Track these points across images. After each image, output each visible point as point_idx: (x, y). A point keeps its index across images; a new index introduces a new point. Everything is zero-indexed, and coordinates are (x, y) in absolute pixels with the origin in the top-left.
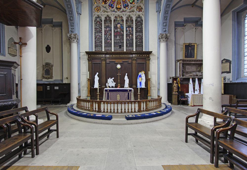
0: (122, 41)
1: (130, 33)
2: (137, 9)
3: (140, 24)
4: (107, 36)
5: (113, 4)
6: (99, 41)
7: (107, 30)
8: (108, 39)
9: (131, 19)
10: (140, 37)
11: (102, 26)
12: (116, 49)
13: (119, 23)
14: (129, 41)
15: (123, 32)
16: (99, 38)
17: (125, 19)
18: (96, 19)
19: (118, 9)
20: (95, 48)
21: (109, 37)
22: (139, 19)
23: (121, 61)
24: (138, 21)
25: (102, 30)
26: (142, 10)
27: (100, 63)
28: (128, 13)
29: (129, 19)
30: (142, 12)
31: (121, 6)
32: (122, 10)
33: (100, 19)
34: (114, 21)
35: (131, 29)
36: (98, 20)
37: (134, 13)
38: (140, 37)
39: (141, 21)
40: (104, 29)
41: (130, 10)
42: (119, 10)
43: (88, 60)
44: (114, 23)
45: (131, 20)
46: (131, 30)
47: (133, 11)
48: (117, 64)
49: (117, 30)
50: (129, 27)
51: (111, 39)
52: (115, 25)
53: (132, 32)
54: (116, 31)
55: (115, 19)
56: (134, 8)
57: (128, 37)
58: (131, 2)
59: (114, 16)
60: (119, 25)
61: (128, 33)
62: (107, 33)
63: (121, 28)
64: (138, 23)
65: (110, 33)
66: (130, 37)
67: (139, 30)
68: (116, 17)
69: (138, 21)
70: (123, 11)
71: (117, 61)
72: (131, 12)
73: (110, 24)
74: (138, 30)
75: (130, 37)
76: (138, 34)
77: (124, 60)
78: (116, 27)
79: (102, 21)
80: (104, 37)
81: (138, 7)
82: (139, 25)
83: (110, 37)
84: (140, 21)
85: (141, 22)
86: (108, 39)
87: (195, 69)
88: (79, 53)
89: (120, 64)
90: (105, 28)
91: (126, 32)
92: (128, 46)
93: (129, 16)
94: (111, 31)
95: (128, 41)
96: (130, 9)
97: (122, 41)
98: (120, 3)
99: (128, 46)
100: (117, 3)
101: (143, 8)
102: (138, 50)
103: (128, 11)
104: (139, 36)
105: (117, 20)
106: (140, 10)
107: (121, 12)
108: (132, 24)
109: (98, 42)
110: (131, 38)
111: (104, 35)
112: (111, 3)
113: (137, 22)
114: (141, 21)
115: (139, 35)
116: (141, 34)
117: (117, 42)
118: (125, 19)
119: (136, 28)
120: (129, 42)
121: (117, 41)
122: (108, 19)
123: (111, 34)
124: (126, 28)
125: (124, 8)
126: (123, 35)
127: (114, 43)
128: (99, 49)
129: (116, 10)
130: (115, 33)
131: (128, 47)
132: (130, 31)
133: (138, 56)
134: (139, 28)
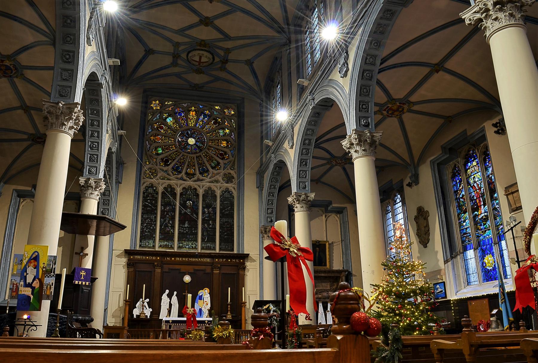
1: (209, 217)
2: (223, 178)
4: (166, 220)
5: (181, 166)
7: (166, 210)
8: (166, 226)
9: (212, 194)
10: (228, 226)
13: (189, 200)
14: (207, 231)
15: (197, 214)
17: (201, 192)
18: (147, 190)
19: (190, 176)
20: (141, 241)
21: (170, 223)
22: (226, 195)
23: (191, 268)
26: (233, 180)
27: (151, 272)
28: (208, 184)
29: (210, 194)
30: (233, 183)
31: (194, 170)
32: (195, 178)
34: (181, 194)
35: (213, 211)
36: (150, 190)
37: (218, 185)
39: (231, 197)
40: (161, 208)
41: (210, 178)
46: (212, 212)
47: (217, 181)
48: (185, 274)
51: (173, 227)
54: (183, 212)
55: (182, 191)
56: (218, 176)
57: (206, 225)
58: (213, 165)
59: (181, 187)
60: (191, 202)
61: (205, 217)
63: (193, 208)
66: (210, 225)
70: (198, 180)
71: (183, 268)
72: (212, 182)
76: (224, 220)
77: (197, 268)
81: (225, 174)
87: (329, 286)
88: (111, 250)
89: (189, 274)
90: (162, 205)
93: (210, 188)
95: (205, 231)
96: (210, 178)
97: (193, 231)
98: (194, 166)
100: (188, 165)
101: (235, 176)
102: (225, 248)
103: (209, 180)
105: (187, 193)
106: (229, 179)
107: (195, 181)
110: (211, 226)
112: (177, 164)
114: (231, 199)
115: (226, 222)
118: (201, 192)
120: (208, 233)
122: (170, 191)
123: (173, 218)
124: (203, 208)
126: (196, 222)
127: (179, 233)
131: (206, 242)
133: (223, 260)
134: (226, 209)
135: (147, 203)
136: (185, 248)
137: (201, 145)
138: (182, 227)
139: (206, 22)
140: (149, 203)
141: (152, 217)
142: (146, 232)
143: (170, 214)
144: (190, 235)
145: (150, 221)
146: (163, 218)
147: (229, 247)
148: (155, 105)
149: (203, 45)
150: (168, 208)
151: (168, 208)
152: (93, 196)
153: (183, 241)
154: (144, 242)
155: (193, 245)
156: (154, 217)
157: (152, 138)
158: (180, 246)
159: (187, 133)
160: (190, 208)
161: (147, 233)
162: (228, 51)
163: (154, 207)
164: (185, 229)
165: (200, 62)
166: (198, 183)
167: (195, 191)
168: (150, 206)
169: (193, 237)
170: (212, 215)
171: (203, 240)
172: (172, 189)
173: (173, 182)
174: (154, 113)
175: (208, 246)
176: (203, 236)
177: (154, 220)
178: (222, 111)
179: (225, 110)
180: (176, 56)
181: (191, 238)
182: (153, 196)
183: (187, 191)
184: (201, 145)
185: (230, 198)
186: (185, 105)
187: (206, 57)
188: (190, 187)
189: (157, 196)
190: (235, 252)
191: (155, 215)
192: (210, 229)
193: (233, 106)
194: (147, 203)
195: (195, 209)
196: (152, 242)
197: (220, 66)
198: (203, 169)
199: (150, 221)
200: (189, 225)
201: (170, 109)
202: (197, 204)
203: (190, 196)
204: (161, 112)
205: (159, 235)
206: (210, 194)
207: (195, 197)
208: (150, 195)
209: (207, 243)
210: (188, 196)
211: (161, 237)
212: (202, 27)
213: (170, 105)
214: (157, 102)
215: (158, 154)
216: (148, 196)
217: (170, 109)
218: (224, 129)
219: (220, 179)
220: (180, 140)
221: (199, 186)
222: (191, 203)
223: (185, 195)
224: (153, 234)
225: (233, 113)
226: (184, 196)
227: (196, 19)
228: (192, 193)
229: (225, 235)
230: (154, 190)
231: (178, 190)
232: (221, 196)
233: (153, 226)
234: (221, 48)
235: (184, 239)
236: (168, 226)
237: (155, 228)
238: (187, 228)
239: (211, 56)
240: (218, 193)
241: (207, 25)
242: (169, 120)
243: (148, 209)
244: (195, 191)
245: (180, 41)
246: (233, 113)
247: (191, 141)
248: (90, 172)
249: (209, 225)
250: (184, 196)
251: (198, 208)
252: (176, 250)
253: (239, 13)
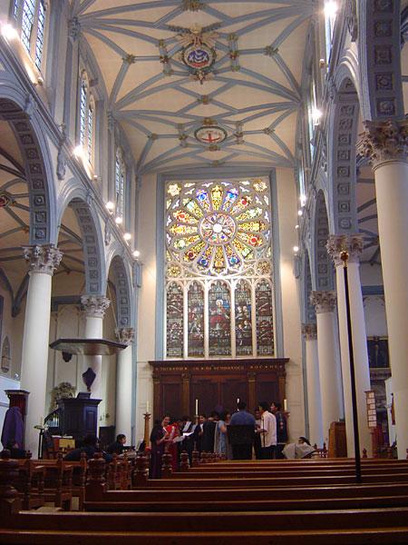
1: (243, 316)
11: (182, 304)
13: (219, 298)
14: (242, 333)
15: (229, 315)
17: (233, 287)
19: (219, 269)
22: (263, 288)
27: (178, 385)
32: (225, 271)
33: (179, 291)
34: (210, 293)
36: (175, 291)
42: (219, 270)
43: (154, 377)
50: (242, 304)
64: (261, 295)
68: (213, 285)
70: (229, 272)
72: (244, 274)
76: (261, 319)
78: (213, 306)
79: (182, 294)
86: (195, 331)
88: (135, 363)
91: (236, 315)
94: (203, 314)
103: (240, 272)
107: (225, 275)
116: (268, 319)
118: (233, 287)
119: (257, 307)
124: (236, 306)
125: (231, 265)
126: (229, 322)
127: (210, 338)
129: (213, 272)
132: (243, 312)
137: (229, 231)
139: (205, 100)
148: (173, 190)
149: (208, 123)
150: (196, 310)
151: (196, 310)
152: (96, 315)
157: (173, 229)
159: (212, 219)
162: (239, 124)
165: (210, 140)
166: (229, 277)
168: (176, 310)
171: (237, 344)
173: (198, 279)
174: (173, 199)
178: (251, 187)
179: (256, 186)
180: (183, 137)
184: (229, 231)
186: (207, 186)
187: (216, 135)
188: (219, 281)
190: (276, 357)
193: (263, 178)
197: (235, 139)
198: (234, 261)
201: (191, 192)
204: (180, 198)
206: (243, 289)
212: (202, 105)
213: (192, 187)
214: (176, 186)
215: (180, 248)
216: (172, 298)
217: (191, 192)
218: (254, 208)
219: (255, 269)
220: (204, 228)
225: (265, 187)
227: (193, 100)
230: (179, 291)
231: (207, 287)
232: (256, 292)
234: (230, 122)
239: (222, 132)
240: (253, 287)
241: (206, 103)
242: (191, 206)
245: (182, 122)
246: (265, 187)
247: (217, 228)
248: (92, 290)
249: (244, 326)
252: (207, 358)
253: (238, 87)
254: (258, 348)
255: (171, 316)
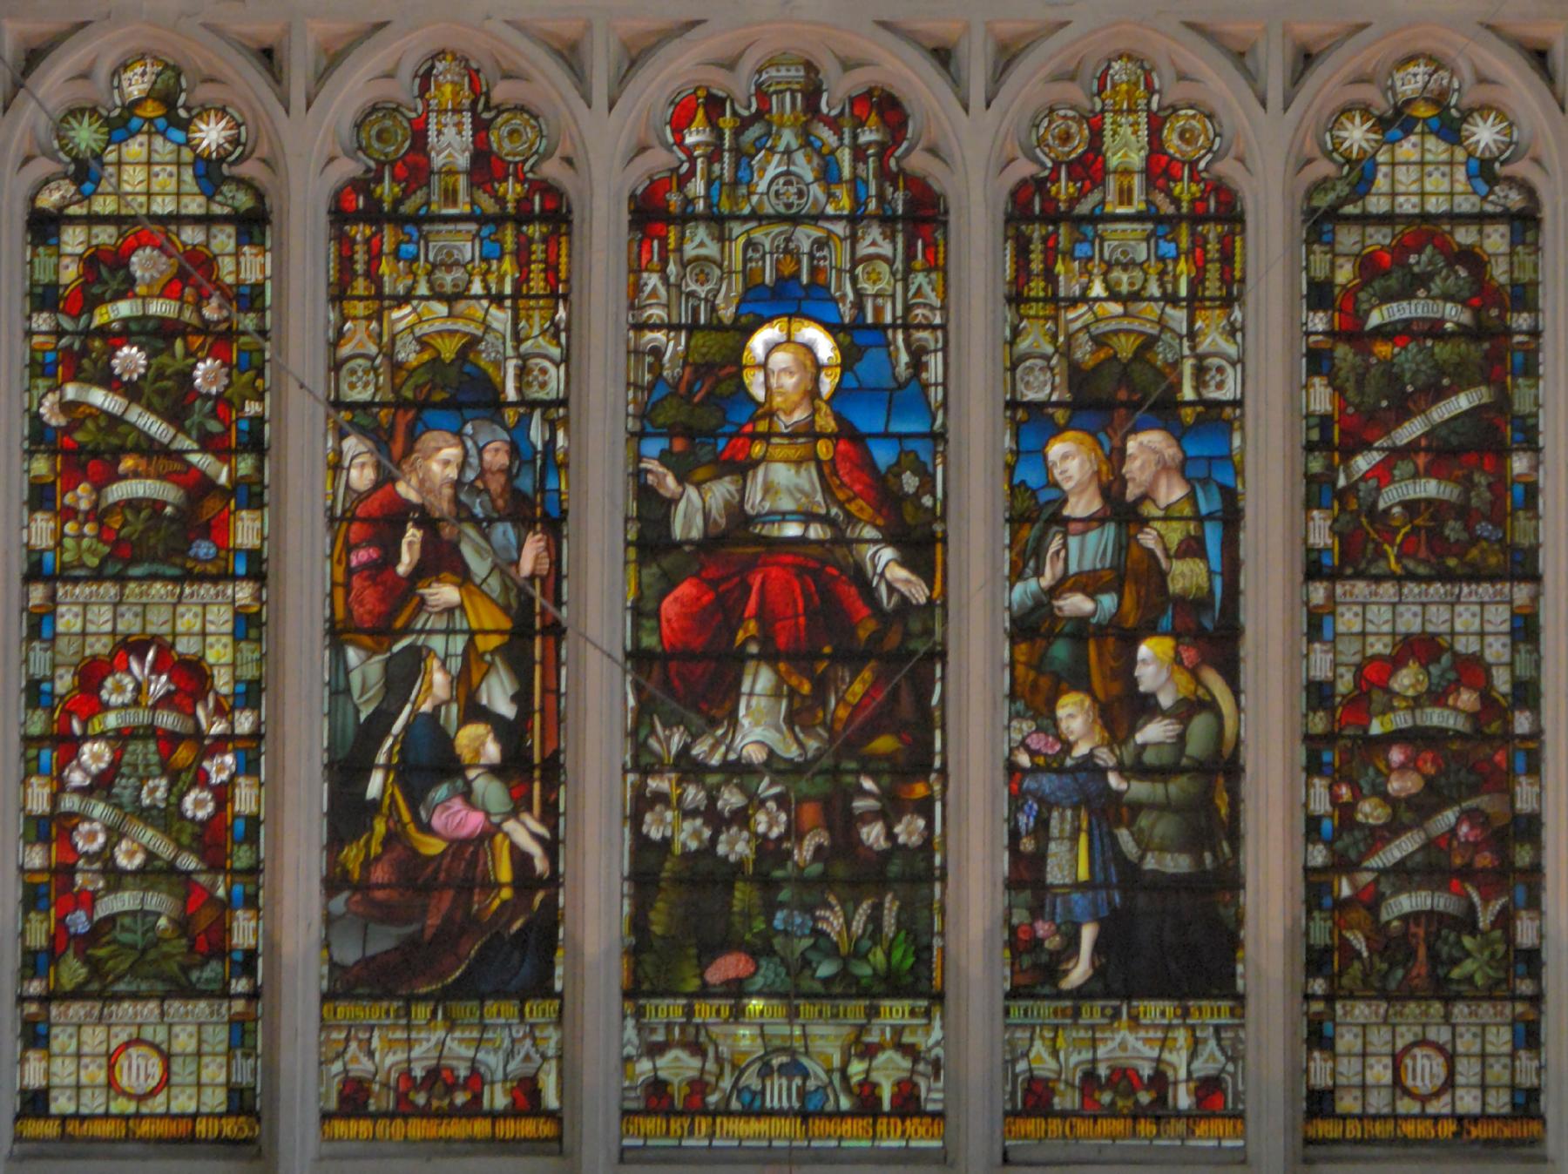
0: (890, 812)
3: (1454, 314)
4: (415, 661)
6: (168, 818)
7: (407, 490)
9: (1159, 169)
10: (1435, 717)
12: (678, 1066)
16: (167, 720)
18: (84, 172)
21: (474, 711)
24: (1380, 237)
25: (251, 494)
38: (1437, 697)
39: (1480, 219)
44: (636, 270)
45: (1185, 189)
46: (1172, 492)
49: (720, 491)
52: (672, 346)
53: (1193, 548)
54: (687, 522)
55: (659, 160)
57: (1073, 714)
61: (1062, 585)
62: (427, 570)
65: (505, 565)
67: (1429, 488)
69: (1387, 219)
73: (500, 318)
74: (1391, 497)
75: (1146, 707)
80: (339, 690)
82: (1435, 330)
83: (499, 695)
84: (1455, 218)
85: (1473, 259)
91: (1026, 559)
92: (1079, 972)
97: (873, 834)
99: (1079, 972)
104: (1406, 680)
108: (1195, 302)
109: (127, 859)
110: (1154, 732)
111: (338, 635)
113: (1369, 266)
115: (1420, 647)
117: (736, 846)
120: (1105, 851)
121: (741, 818)
128: (139, 1070)
130: (669, 582)
131: (1081, 994)
134: (1411, 430)
135: (99, 397)
136: (748, 1113)
138: (689, 769)
140: (131, 391)
141: (188, 620)
142: (116, 878)
143: (479, 566)
144: (813, 890)
145: (160, 685)
146: (381, 632)
147: (1467, 1071)
153: (705, 992)
154: (94, 1039)
155: (869, 1052)
156: (221, 618)
158: (657, 1087)
160: (809, 432)
161: (125, 901)
163: (223, 452)
164: (731, 799)
167: (884, 150)
168: (150, 449)
169: (875, 918)
170: (1175, 534)
172: (499, 140)
175: (1123, 1078)
176: (1037, 912)
177: (223, 682)
181: (833, 951)
182: (200, 263)
183: (740, 154)
185: (1464, 236)
189: (251, 276)
191: (244, 593)
192: (1140, 789)
194: (99, 397)
195: (883, 455)
196: (218, 1037)
199: (166, 701)
200: (796, 719)
202: (917, 365)
203: (805, 237)
205: (329, 920)
207: (874, 241)
208: (144, 264)
209: (1093, 1012)
210: (766, 236)
211: (349, 954)
221: (943, 56)
222: (826, 348)
223: (717, 221)
224: (227, 905)
226: (699, 242)
228: (828, 174)
229: (1404, 875)
233: (221, 767)
235: (728, 967)
236: (449, 766)
237: (245, 799)
238: (767, 788)
243: (118, 491)
244: (884, 150)
250: (699, 242)
251: (938, 438)
254: (1319, 1038)
255: (83, 542)
